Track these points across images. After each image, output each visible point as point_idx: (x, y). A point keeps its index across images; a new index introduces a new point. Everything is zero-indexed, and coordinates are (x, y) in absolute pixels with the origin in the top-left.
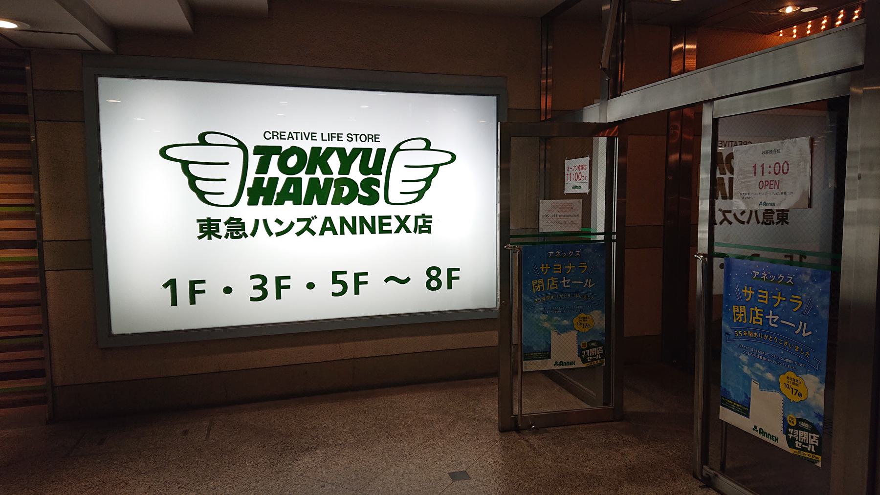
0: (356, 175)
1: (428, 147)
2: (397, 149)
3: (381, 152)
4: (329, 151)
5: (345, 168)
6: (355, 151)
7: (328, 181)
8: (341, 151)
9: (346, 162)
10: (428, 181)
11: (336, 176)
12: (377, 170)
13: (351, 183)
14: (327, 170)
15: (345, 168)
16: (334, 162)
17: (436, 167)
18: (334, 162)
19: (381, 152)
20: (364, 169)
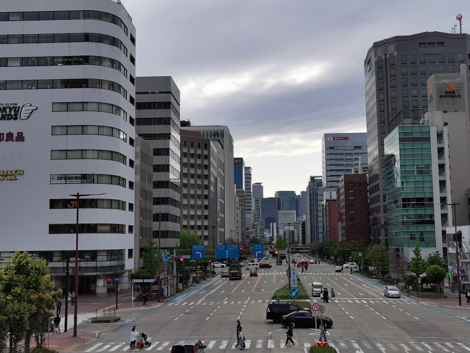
0: (13, 113)
1: (31, 105)
2: (23, 106)
3: (19, 107)
4: (7, 107)
5: (10, 111)
6: (13, 107)
7: (6, 114)
8: (10, 107)
9: (11, 109)
10: (31, 113)
11: (8, 113)
12: (18, 111)
13: (11, 115)
14: (6, 112)
15: (10, 111)
16: (8, 110)
17: (33, 110)
18: (8, 110)
19: (19, 107)
20: (15, 111)
